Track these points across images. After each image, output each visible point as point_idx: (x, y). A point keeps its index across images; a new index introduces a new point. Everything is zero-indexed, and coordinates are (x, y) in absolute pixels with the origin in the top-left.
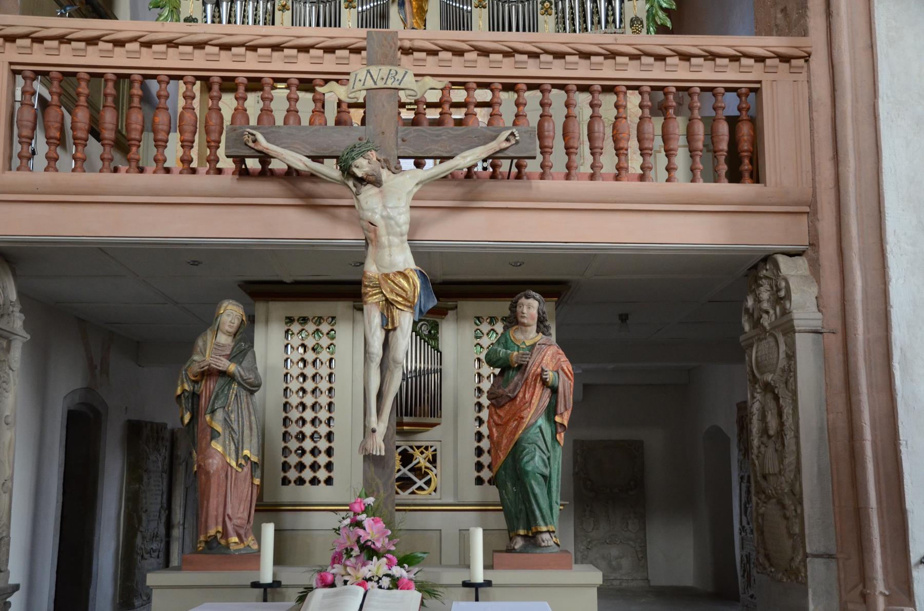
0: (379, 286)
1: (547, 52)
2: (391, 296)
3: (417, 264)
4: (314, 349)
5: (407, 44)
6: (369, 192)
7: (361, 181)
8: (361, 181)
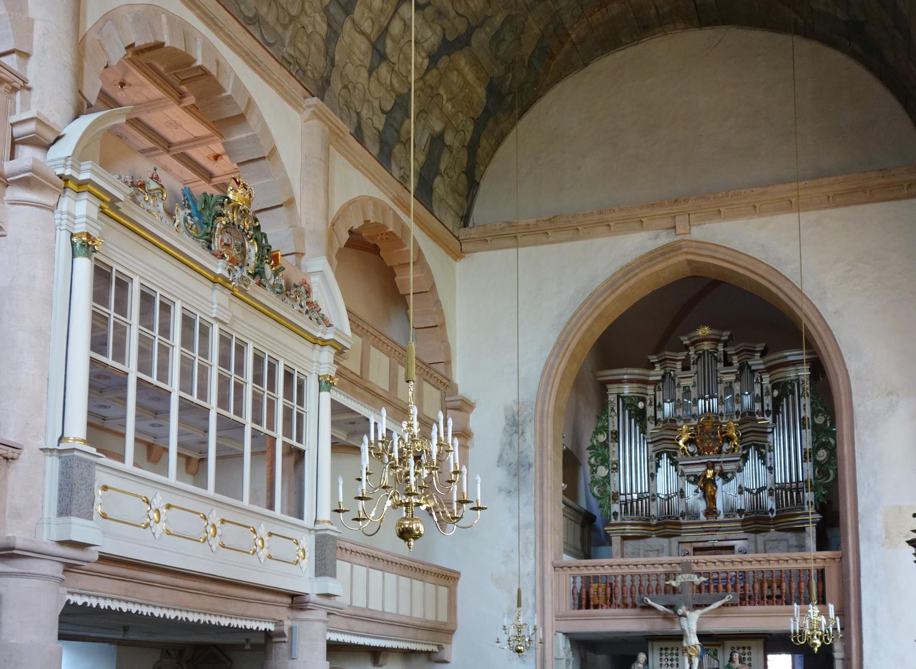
0: (686, 650)
1: (745, 561)
2: (691, 654)
3: (700, 641)
4: (671, 660)
5: (696, 561)
6: (683, 619)
7: (681, 616)
8: (681, 616)
